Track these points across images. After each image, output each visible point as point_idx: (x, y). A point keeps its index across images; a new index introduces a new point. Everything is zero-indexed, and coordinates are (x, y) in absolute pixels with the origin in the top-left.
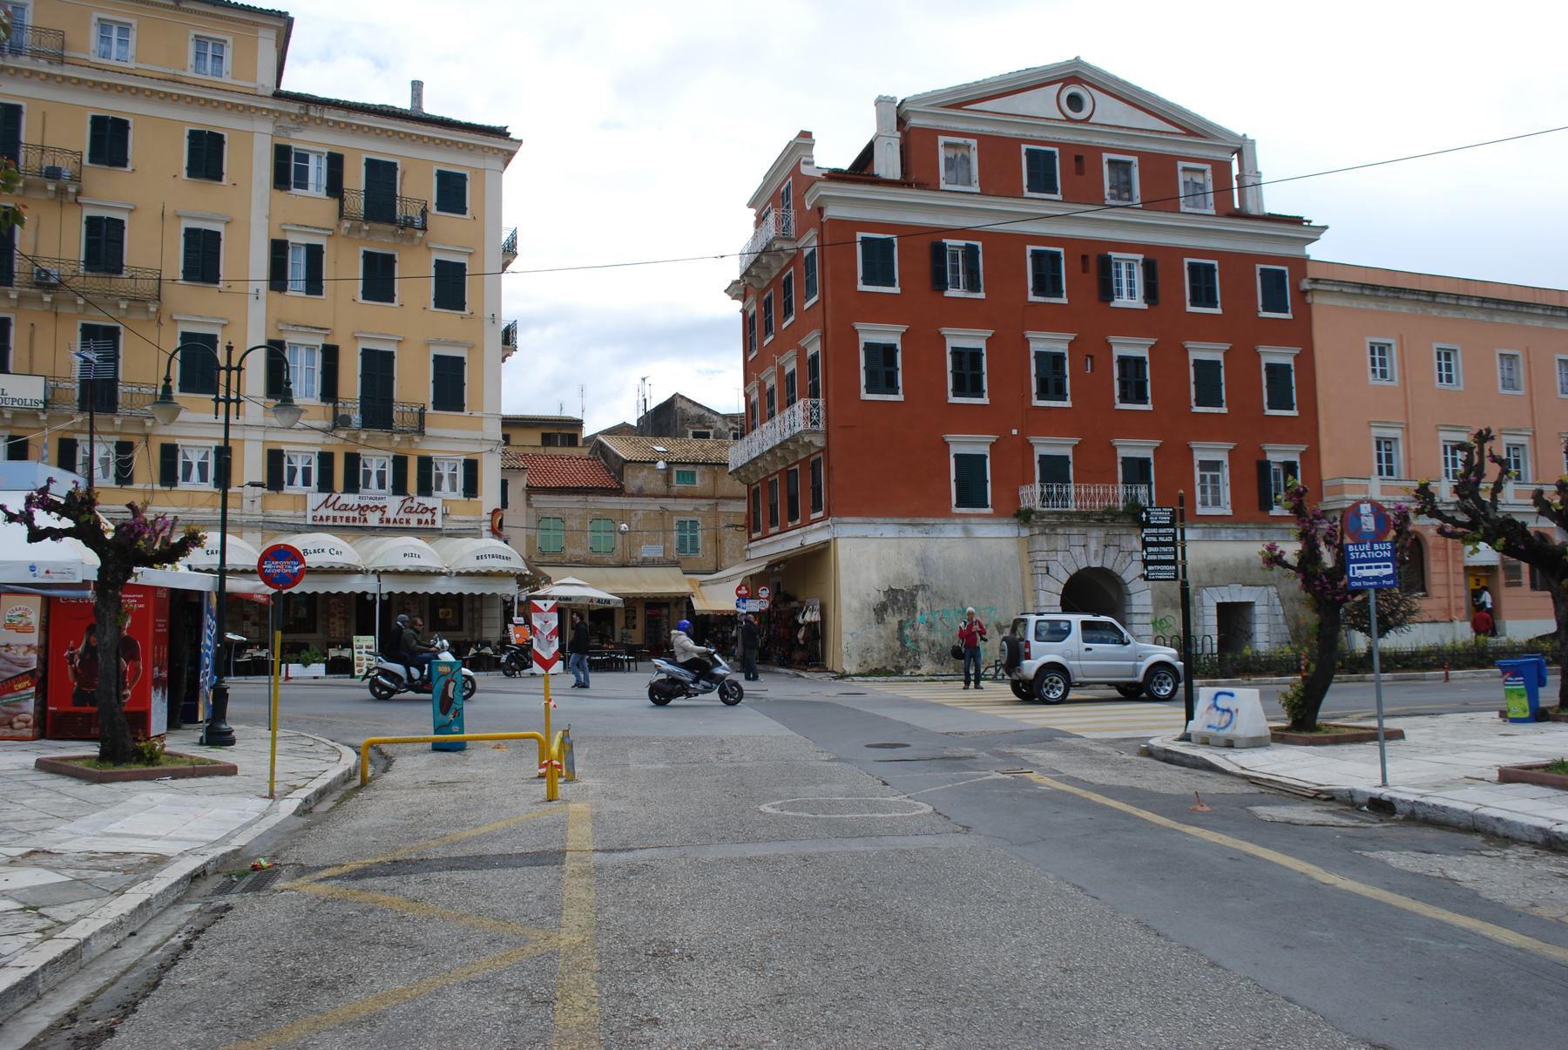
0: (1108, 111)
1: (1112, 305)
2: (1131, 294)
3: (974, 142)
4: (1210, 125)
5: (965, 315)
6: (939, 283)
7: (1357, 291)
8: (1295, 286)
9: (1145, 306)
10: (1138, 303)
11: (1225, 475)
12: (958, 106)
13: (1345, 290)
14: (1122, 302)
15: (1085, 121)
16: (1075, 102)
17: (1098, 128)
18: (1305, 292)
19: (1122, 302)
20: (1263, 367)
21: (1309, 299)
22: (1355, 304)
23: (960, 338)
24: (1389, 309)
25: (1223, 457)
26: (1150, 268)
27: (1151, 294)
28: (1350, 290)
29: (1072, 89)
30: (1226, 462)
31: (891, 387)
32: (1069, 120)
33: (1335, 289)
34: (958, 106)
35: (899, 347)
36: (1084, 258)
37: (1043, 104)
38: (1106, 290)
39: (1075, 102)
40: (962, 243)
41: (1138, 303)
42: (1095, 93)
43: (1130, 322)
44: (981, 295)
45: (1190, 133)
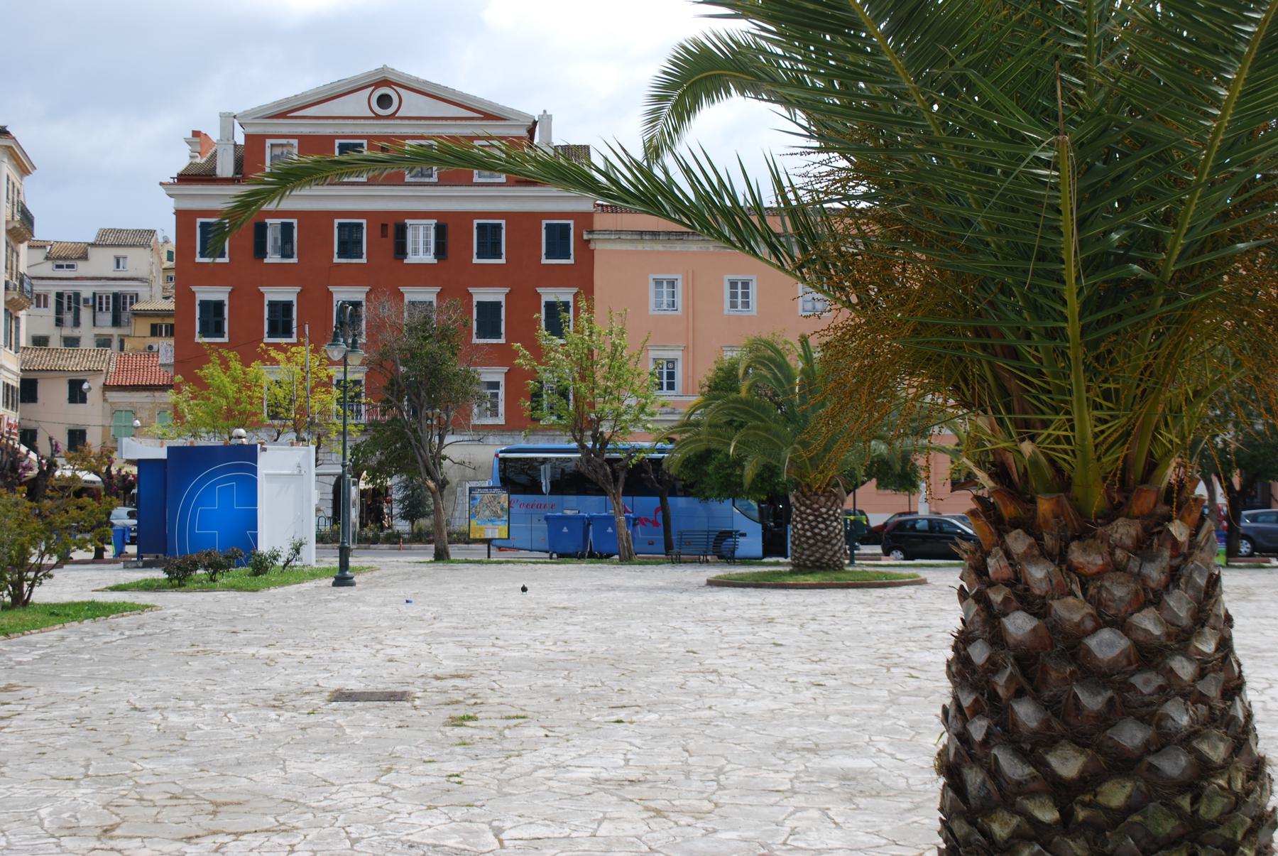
0: (413, 105)
1: (406, 261)
2: (427, 250)
3: (295, 142)
4: (502, 109)
5: (280, 276)
6: (261, 251)
7: (639, 237)
8: (579, 236)
9: (435, 261)
10: (430, 259)
11: (501, 392)
12: (282, 115)
13: (623, 237)
14: (411, 259)
15: (392, 117)
16: (384, 101)
17: (406, 122)
18: (589, 241)
19: (411, 259)
20: (543, 304)
21: (592, 246)
22: (640, 247)
23: (274, 294)
24: (678, 249)
25: (501, 379)
26: (441, 231)
27: (441, 251)
28: (629, 237)
29: (384, 90)
30: (502, 383)
31: (219, 332)
32: (378, 117)
33: (613, 237)
34: (282, 115)
35: (227, 303)
36: (384, 226)
37: (358, 105)
38: (401, 250)
39: (384, 101)
40: (279, 221)
41: (430, 259)
42: (402, 91)
43: (420, 275)
44: (294, 260)
45: (488, 116)
